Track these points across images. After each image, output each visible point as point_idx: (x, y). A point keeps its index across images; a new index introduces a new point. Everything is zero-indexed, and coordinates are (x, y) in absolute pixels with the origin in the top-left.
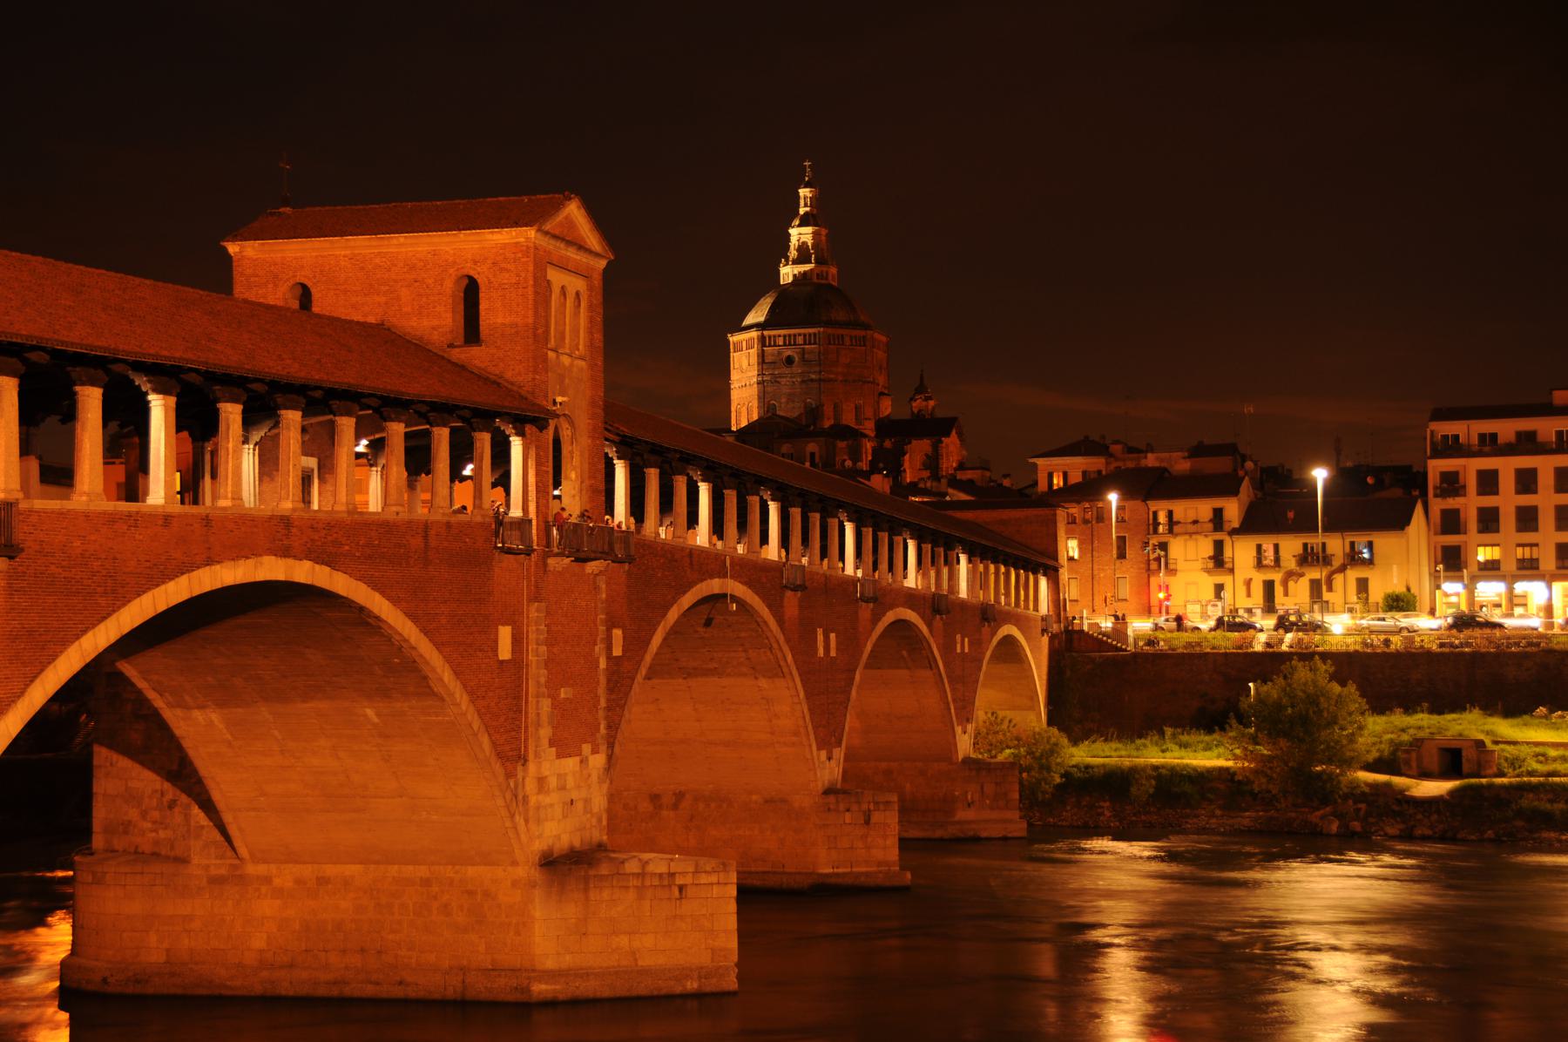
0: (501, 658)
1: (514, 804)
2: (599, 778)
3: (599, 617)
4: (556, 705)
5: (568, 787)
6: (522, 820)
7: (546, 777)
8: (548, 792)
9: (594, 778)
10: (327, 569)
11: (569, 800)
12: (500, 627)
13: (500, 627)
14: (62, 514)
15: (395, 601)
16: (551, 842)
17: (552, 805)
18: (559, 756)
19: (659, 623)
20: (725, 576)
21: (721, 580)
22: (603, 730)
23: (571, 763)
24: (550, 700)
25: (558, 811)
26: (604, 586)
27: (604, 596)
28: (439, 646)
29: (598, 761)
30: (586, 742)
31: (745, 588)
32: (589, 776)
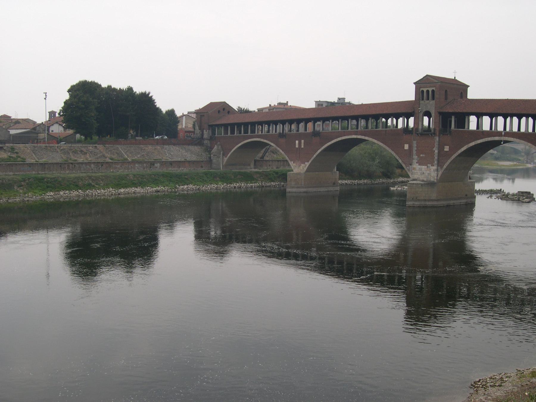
0: (405, 149)
1: (408, 171)
2: (434, 170)
3: (435, 144)
4: (419, 156)
5: (423, 170)
6: (410, 174)
7: (415, 168)
8: (416, 170)
9: (432, 170)
10: (364, 136)
11: (423, 172)
12: (405, 145)
13: (405, 145)
14: (269, 134)
15: (378, 140)
16: (416, 178)
17: (417, 172)
18: (419, 165)
19: (466, 145)
20: (502, 136)
21: (500, 137)
22: (436, 162)
23: (424, 167)
24: (417, 156)
25: (419, 174)
26: (438, 138)
27: (438, 140)
28: (389, 147)
29: (435, 167)
30: (429, 164)
31: (515, 139)
32: (430, 169)
